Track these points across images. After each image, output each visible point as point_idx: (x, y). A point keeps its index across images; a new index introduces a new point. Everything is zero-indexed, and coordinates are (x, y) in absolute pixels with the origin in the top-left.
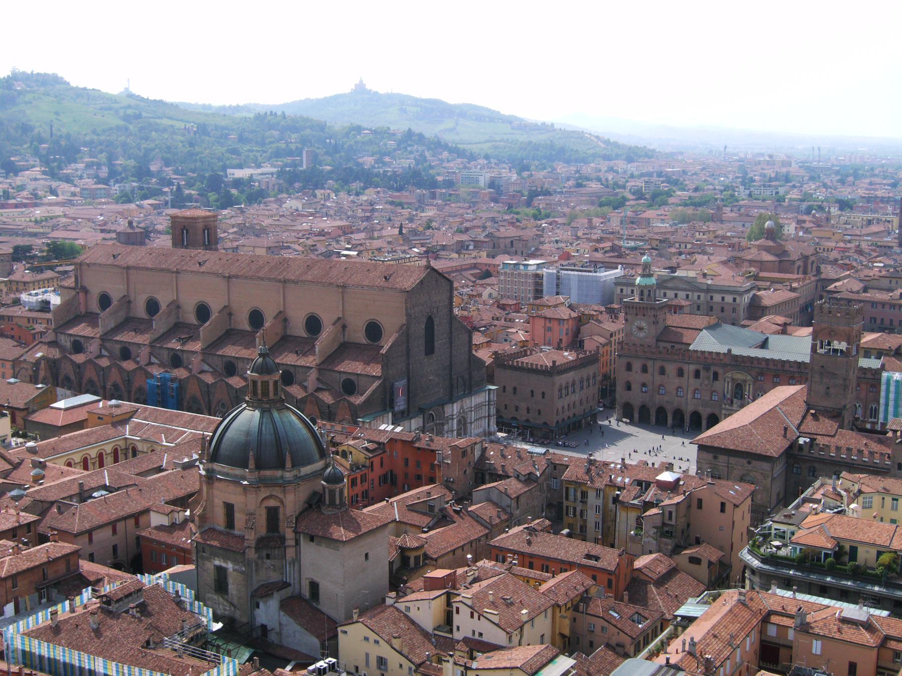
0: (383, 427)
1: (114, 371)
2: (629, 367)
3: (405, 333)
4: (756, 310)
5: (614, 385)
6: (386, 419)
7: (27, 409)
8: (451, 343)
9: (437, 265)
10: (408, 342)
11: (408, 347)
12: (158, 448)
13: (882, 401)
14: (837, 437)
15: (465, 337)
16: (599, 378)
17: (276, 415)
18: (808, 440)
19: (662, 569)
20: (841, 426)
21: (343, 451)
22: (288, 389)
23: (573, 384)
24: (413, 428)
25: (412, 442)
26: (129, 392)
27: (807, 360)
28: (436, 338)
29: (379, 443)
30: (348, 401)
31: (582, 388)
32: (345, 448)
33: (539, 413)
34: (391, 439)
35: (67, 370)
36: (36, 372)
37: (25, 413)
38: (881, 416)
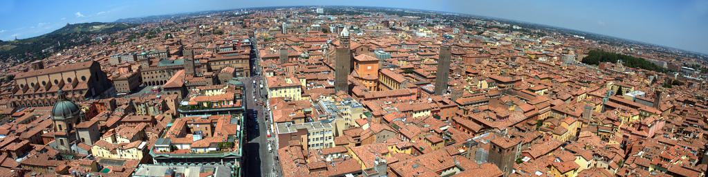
3: (91, 78)
4: (169, 55)
9: (95, 60)
19: (161, 118)
35: (17, 103)
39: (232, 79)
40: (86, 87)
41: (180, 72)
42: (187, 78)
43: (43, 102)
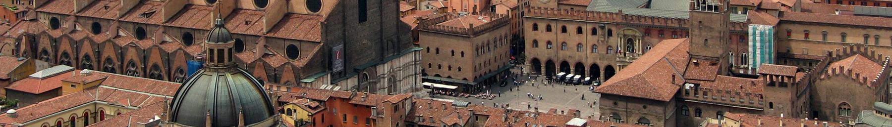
0: (323, 87)
1: (86, 43)
2: (535, 27)
5: (523, 43)
6: (325, 81)
7: (9, 79)
8: (381, 11)
10: (344, 12)
11: (344, 16)
12: (123, 111)
13: (750, 49)
14: (717, 82)
15: (393, 5)
16: (509, 38)
17: (230, 77)
18: (693, 85)
20: (719, 73)
21: (289, 109)
22: (238, 55)
23: (488, 44)
24: (349, 88)
25: (350, 99)
26: (99, 62)
27: (687, 16)
28: (368, 7)
29: (320, 101)
30: (292, 65)
31: (496, 46)
32: (290, 107)
33: (460, 70)
34: (331, 98)
35: (44, 44)
36: (18, 46)
37: (7, 83)
38: (751, 62)
39: (870, 107)
40: (316, 36)
41: (667, 46)
42: (694, 73)
43: (145, 60)
